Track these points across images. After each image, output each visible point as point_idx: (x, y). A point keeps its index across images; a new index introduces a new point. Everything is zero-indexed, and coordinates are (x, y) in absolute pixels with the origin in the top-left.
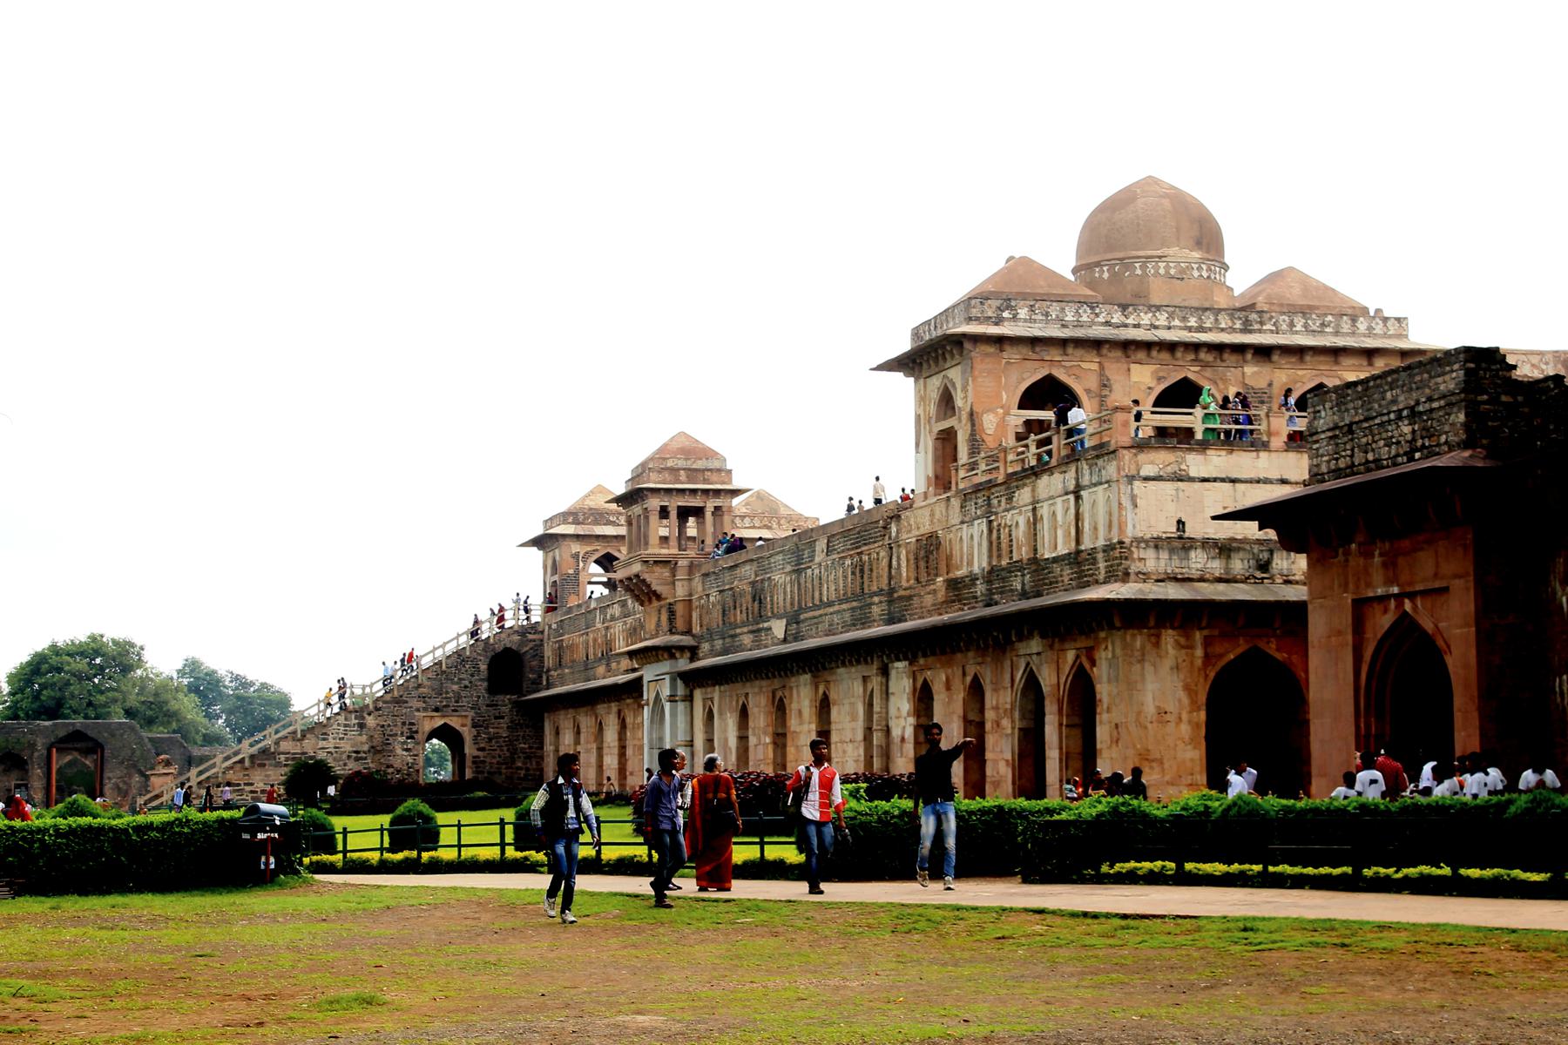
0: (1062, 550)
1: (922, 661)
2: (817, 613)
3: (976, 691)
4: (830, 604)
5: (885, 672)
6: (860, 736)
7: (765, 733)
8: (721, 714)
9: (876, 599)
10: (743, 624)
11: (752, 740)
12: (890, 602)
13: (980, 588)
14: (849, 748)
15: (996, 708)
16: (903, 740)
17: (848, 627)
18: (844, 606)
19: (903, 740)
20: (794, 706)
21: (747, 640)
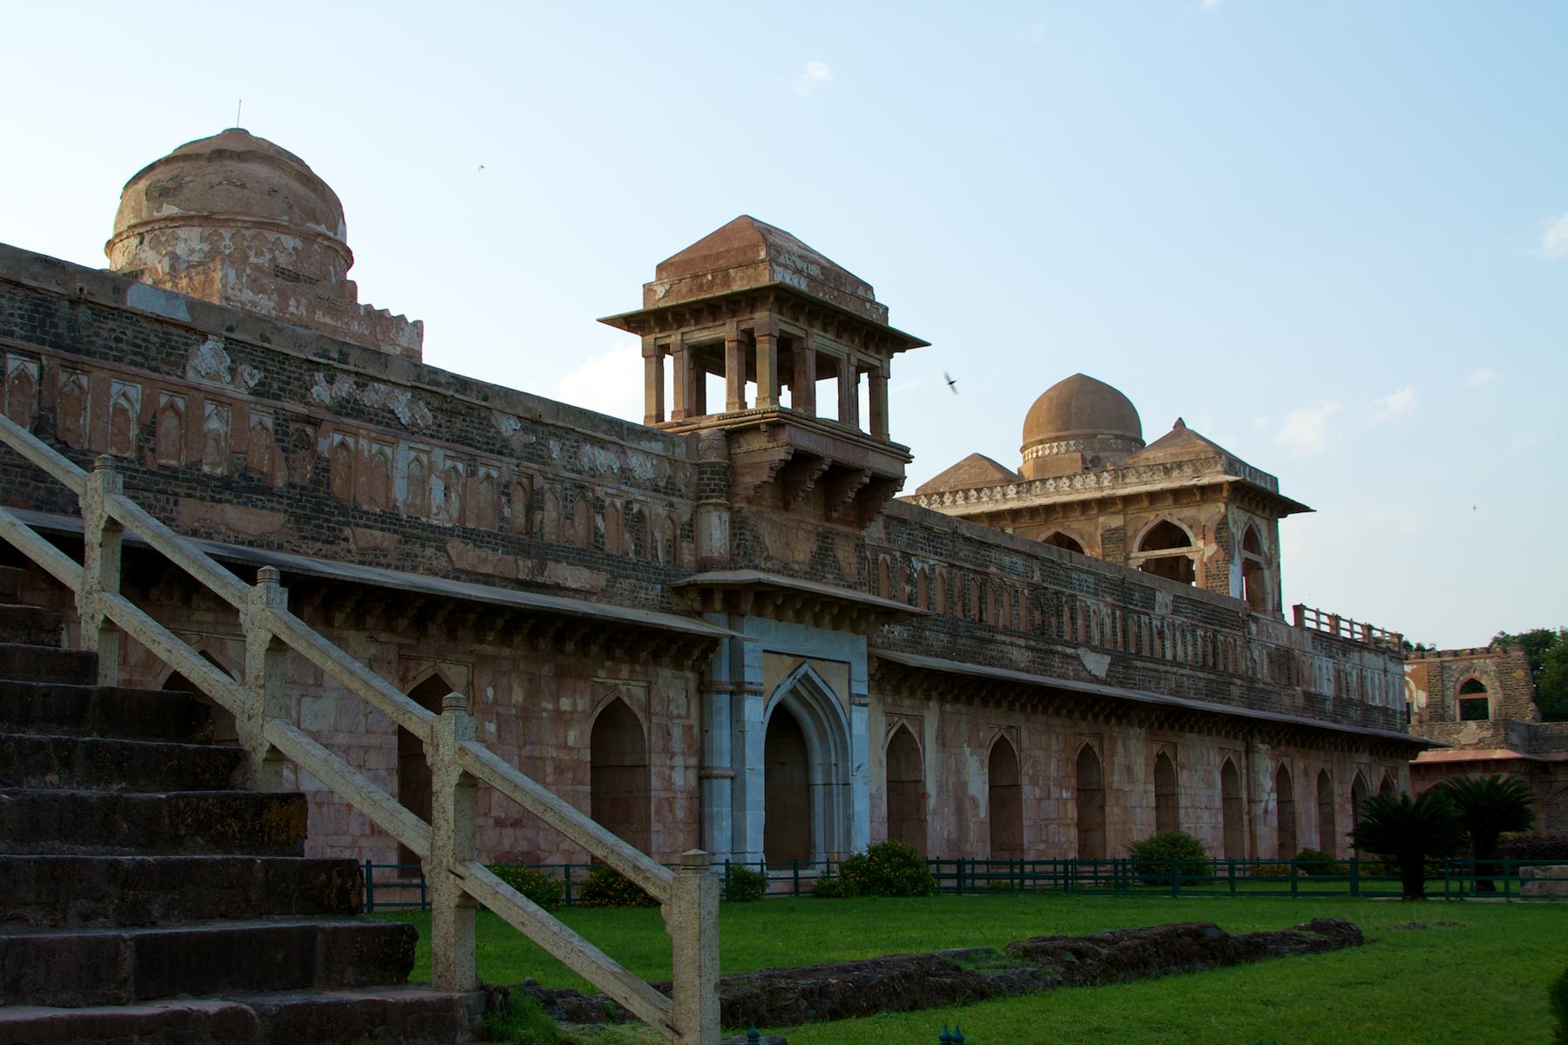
0: (1377, 703)
1: (1283, 748)
2: (1161, 668)
3: (1323, 778)
4: (1175, 662)
5: (1249, 750)
6: (1218, 803)
7: (1060, 785)
8: (943, 742)
9: (1238, 682)
10: (1007, 631)
11: (1029, 792)
12: (1250, 689)
13: (1329, 707)
14: (1206, 815)
15: (1341, 796)
16: (1266, 811)
17: (1198, 695)
18: (1200, 674)
19: (1266, 811)
20: (1119, 759)
21: (1020, 656)
